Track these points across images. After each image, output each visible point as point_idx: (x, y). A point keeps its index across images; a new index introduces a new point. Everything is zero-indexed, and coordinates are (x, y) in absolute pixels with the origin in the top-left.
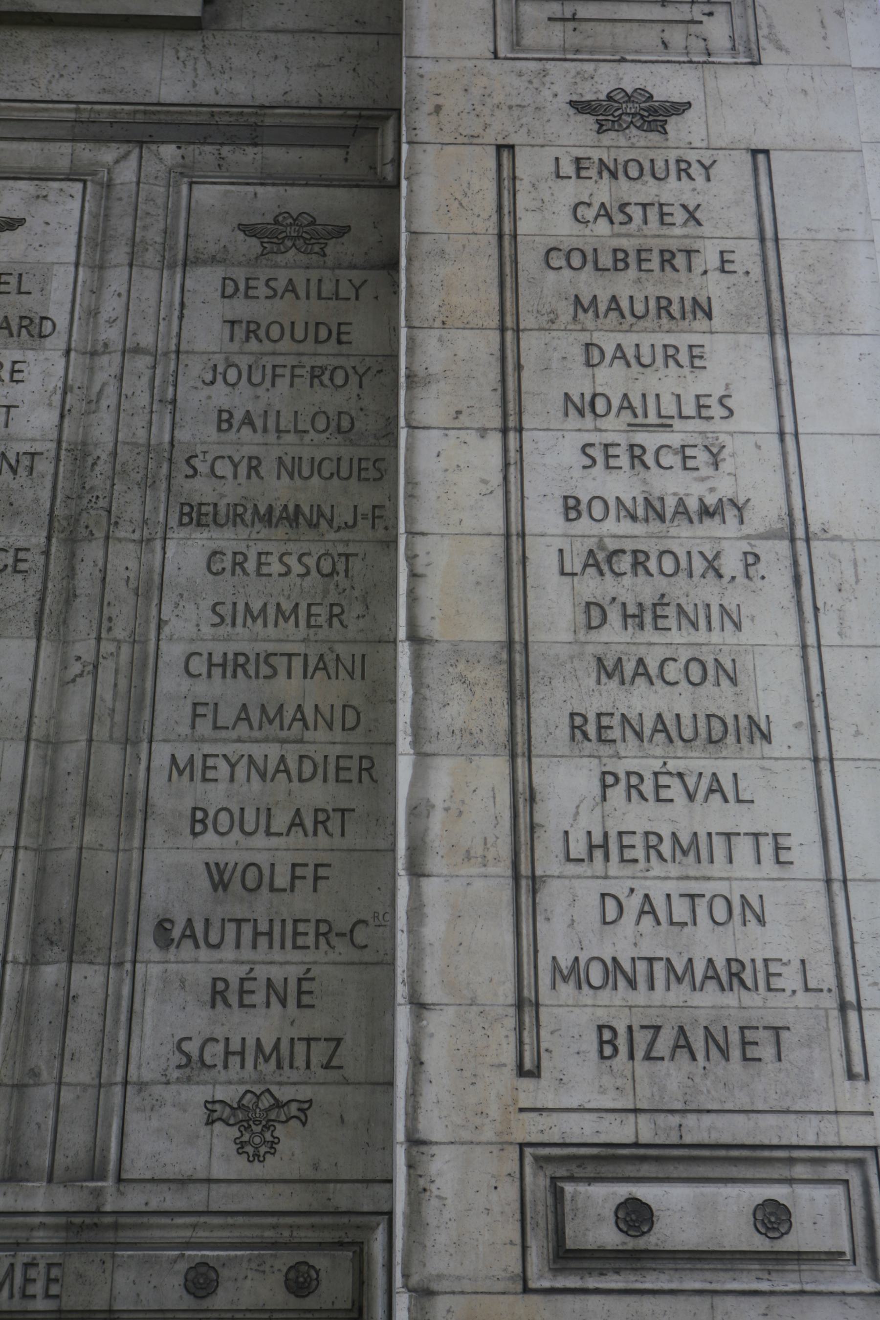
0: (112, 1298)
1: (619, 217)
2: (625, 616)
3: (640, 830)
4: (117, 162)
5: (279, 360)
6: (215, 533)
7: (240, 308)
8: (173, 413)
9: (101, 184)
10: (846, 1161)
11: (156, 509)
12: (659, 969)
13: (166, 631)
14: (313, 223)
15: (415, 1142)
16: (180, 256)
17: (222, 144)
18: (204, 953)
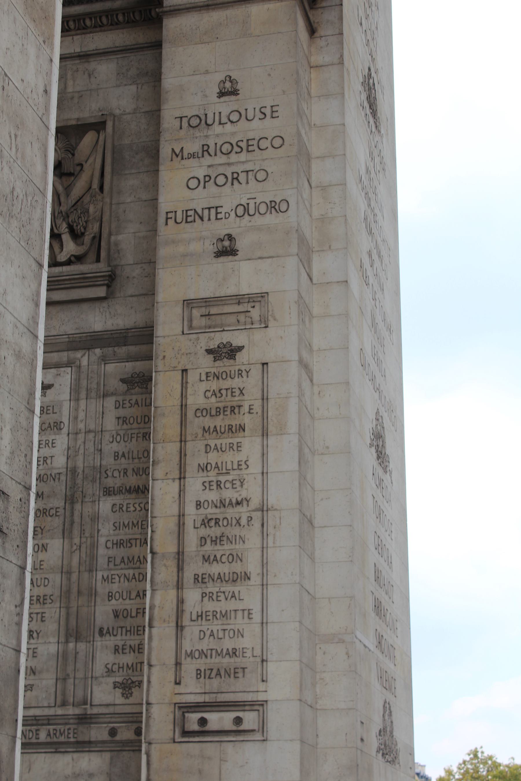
0: (90, 738)
1: (219, 395)
2: (212, 541)
3: (211, 610)
4: (82, 357)
5: (133, 431)
6: (114, 497)
7: (122, 412)
8: (101, 454)
9: (77, 366)
10: (259, 705)
11: (96, 490)
12: (214, 652)
13: (100, 533)
14: (144, 376)
15: (148, 704)
16: (102, 394)
17: (115, 346)
18: (112, 638)
